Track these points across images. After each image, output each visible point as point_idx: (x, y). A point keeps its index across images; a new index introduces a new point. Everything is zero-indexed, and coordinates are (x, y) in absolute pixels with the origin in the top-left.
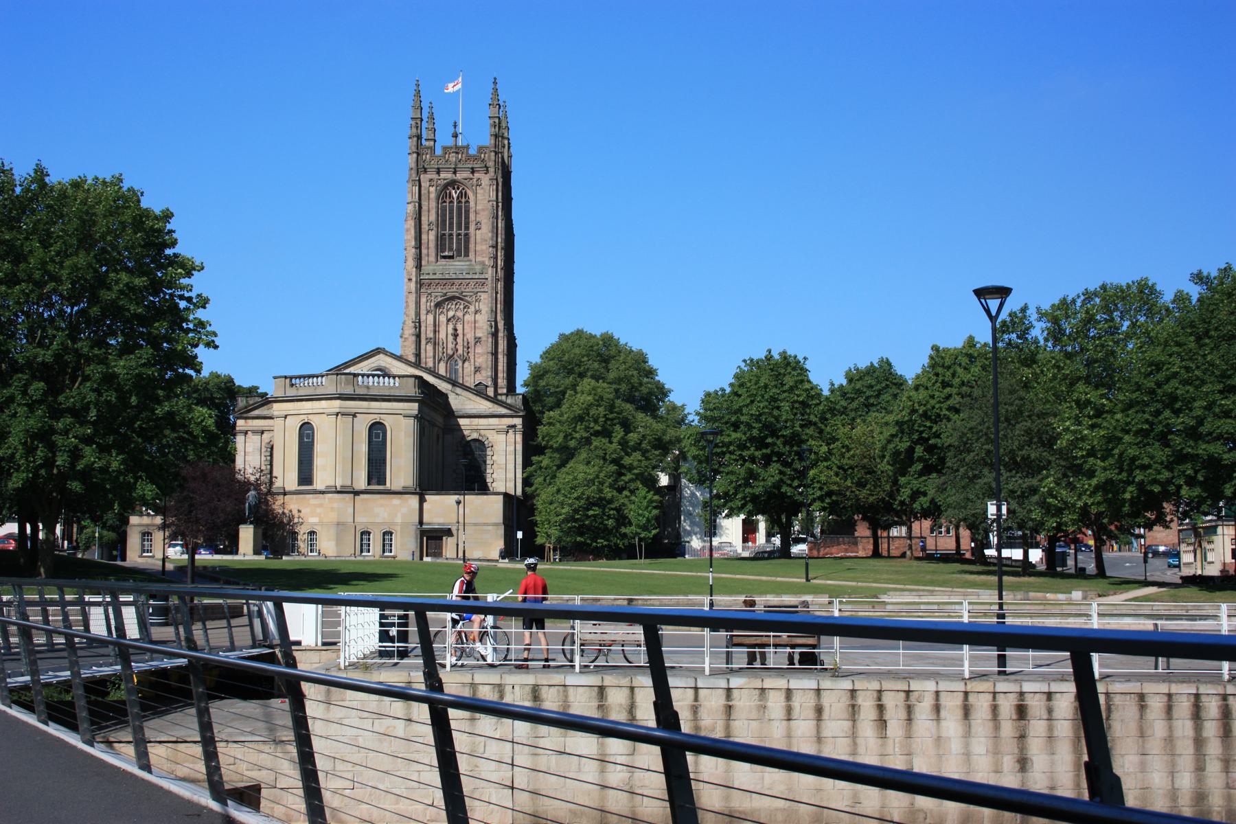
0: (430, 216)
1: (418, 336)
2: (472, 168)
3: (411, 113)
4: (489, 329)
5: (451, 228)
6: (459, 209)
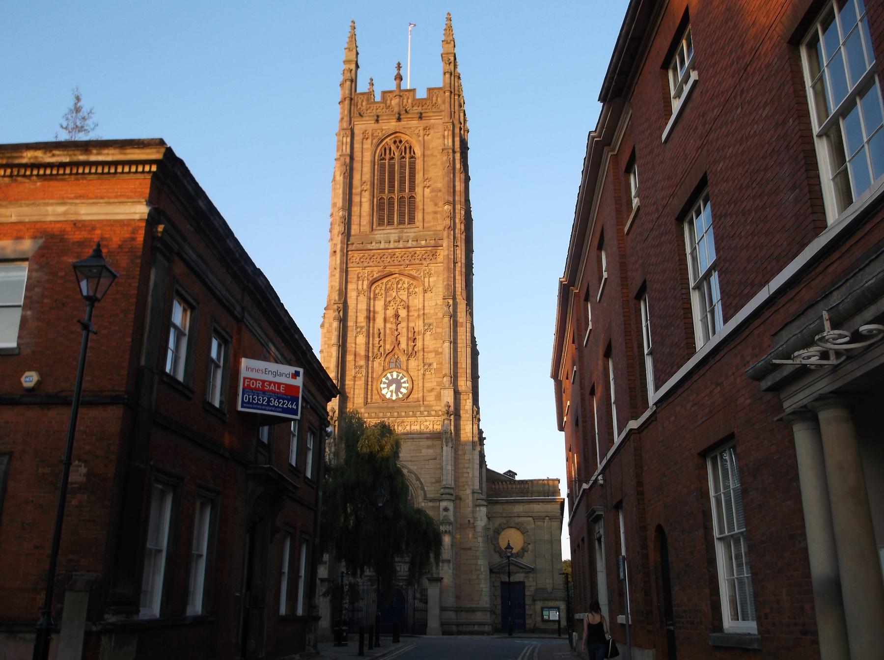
0: (364, 173)
1: (343, 321)
3: (343, 55)
4: (446, 308)
6: (402, 167)
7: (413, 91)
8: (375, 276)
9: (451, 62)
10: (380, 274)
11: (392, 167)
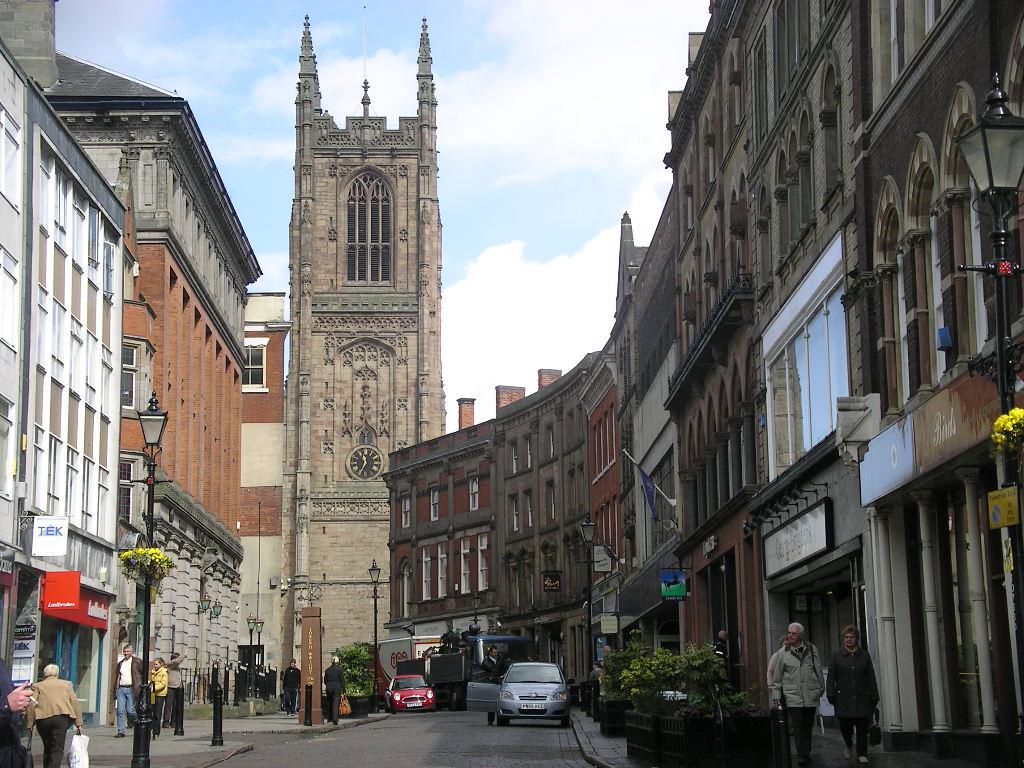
2: (392, 150)
5: (363, 238)
6: (375, 209)
7: (382, 120)
8: (343, 344)
9: (425, 79)
10: (348, 342)
11: (363, 210)
